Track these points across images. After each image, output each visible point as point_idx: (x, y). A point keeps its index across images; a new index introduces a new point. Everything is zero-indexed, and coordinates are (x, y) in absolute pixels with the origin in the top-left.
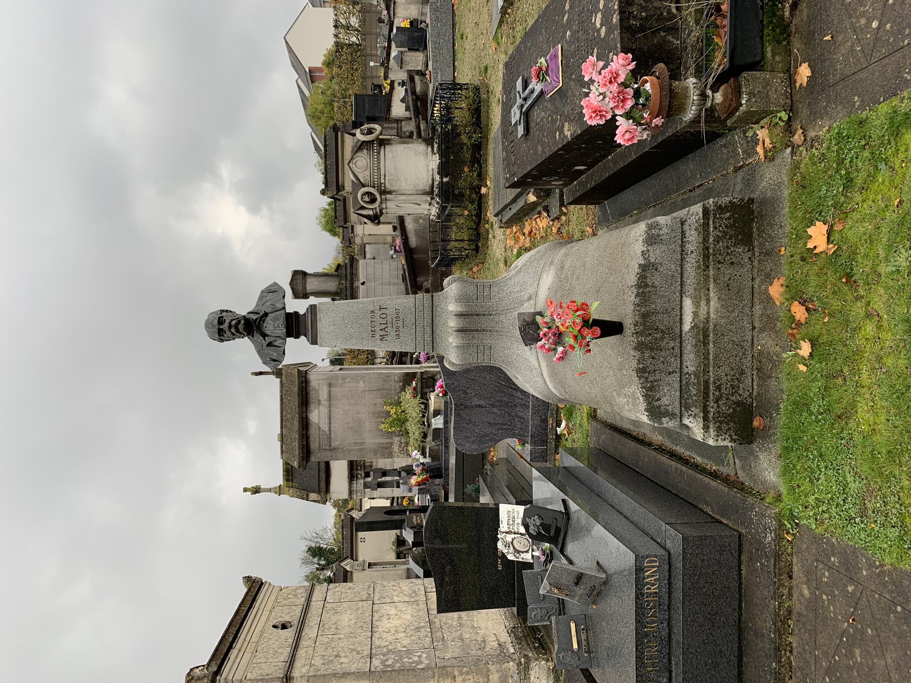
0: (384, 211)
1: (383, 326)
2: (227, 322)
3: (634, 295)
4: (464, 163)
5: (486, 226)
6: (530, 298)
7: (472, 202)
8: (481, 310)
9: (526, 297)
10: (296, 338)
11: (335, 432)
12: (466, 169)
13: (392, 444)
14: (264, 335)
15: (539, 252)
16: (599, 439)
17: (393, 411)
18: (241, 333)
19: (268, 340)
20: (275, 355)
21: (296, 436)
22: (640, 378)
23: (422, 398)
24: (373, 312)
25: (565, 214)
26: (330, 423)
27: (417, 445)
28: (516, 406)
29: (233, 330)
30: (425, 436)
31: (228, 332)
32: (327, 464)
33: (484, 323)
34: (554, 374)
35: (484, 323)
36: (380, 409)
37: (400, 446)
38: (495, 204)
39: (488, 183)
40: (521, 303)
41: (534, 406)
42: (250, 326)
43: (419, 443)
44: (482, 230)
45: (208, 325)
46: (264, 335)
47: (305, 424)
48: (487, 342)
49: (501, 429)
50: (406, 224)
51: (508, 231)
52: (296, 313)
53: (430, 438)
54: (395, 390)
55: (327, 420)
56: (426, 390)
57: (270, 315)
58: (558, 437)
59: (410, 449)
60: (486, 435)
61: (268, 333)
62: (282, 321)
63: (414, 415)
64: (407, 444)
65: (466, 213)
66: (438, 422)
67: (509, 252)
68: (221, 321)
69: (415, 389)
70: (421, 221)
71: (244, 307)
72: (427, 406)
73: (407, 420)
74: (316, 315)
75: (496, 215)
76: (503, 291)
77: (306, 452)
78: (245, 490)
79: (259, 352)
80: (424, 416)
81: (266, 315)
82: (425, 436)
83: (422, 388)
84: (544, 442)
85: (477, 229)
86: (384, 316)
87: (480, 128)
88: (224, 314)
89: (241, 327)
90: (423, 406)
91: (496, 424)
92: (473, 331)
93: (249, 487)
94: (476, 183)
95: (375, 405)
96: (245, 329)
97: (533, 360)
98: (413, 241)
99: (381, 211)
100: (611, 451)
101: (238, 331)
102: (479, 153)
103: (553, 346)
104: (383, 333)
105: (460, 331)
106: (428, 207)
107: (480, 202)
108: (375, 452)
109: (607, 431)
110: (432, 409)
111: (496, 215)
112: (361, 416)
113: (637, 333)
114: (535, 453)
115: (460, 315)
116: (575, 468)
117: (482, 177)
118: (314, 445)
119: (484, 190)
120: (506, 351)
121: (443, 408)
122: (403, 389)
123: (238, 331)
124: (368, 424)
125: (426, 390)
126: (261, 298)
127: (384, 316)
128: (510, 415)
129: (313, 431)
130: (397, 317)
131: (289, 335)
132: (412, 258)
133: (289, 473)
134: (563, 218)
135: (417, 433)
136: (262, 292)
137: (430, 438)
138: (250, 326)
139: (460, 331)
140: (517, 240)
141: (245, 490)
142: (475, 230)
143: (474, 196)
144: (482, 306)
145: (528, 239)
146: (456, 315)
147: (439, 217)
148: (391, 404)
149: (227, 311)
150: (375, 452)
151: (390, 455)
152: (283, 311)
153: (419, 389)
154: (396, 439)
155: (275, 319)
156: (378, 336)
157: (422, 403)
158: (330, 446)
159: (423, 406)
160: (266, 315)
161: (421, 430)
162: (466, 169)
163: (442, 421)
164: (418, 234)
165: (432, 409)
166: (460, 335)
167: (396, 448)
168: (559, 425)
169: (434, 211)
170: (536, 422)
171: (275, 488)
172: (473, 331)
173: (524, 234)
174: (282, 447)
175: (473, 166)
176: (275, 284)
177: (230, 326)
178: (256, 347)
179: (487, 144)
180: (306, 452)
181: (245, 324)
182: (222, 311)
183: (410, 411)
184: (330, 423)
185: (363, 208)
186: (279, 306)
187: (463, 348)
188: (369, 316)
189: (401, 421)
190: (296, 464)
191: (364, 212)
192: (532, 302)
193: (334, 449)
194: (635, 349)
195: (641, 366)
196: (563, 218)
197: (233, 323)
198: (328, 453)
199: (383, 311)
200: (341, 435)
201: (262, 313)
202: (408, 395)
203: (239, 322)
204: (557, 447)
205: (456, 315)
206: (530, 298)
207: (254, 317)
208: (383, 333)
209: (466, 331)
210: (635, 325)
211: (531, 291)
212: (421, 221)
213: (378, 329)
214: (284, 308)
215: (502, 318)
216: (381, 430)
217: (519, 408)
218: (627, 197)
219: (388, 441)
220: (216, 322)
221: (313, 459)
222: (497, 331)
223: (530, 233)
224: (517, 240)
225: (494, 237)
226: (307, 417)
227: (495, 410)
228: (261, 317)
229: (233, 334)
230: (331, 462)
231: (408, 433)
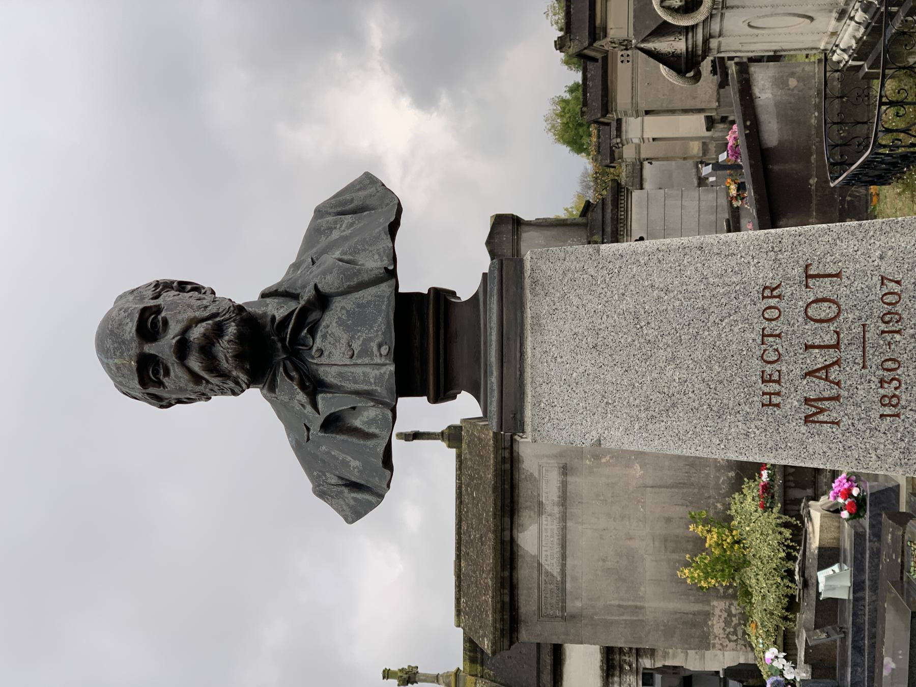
0: (714, 43)
1: (819, 359)
2: (175, 329)
10: (436, 399)
11: (574, 579)
13: (708, 615)
14: (313, 386)
17: (711, 539)
18: (224, 375)
19: (327, 404)
20: (355, 468)
21: (489, 581)
23: (784, 511)
24: (770, 291)
26: (564, 557)
27: (770, 626)
29: (195, 363)
30: (792, 605)
31: (176, 370)
32: (558, 653)
36: (679, 531)
37: (727, 623)
42: (260, 347)
43: (777, 620)
45: (108, 341)
46: (313, 386)
47: (508, 555)
50: (756, 91)
52: (441, 298)
53: (806, 615)
54: (717, 487)
55: (557, 549)
56: (796, 493)
57: (339, 306)
59: (751, 630)
61: (329, 375)
62: (379, 330)
63: (766, 552)
64: (745, 618)
66: (833, 582)
68: (149, 324)
69: (766, 488)
70: (793, 82)
71: (247, 268)
72: (799, 534)
73: (746, 563)
74: (519, 305)
77: (509, 620)
78: (387, 674)
79: (298, 448)
80: (790, 558)
81: (322, 301)
82: (792, 605)
83: (785, 487)
86: (826, 311)
88: (168, 297)
89: (224, 349)
90: (787, 533)
93: (394, 668)
95: (668, 520)
96: (239, 357)
98: (772, 132)
99: (706, 41)
101: (212, 366)
104: (817, 388)
106: (832, 24)
108: (668, 632)
110: (814, 543)
112: (635, 544)
118: (527, 604)
121: (847, 544)
122: (737, 486)
123: (212, 366)
124: (651, 566)
125: (796, 493)
126: (314, 234)
127: (826, 311)
129: (525, 573)
130: (891, 318)
131: (407, 385)
132: (767, 173)
133: (473, 651)
135: (771, 597)
136: (320, 212)
137: (806, 615)
138: (260, 347)
141: (387, 674)
147: (862, 51)
148: (706, 522)
149: (182, 286)
150: (668, 632)
151: (704, 643)
152: (385, 288)
153: (777, 489)
154: (719, 606)
155: (356, 321)
156: (794, 402)
157: (786, 525)
158: (564, 609)
159: (787, 533)
160: (322, 301)
161: (783, 591)
163: (847, 582)
164: (785, 113)
165: (814, 543)
167: (717, 626)
169: (849, 34)
171: (447, 675)
174: (458, 600)
176: (369, 181)
177: (182, 348)
178: (289, 428)
180: (509, 620)
181: (240, 338)
182: (162, 287)
183: (754, 540)
184: (564, 557)
185: (664, 30)
186: (372, 264)
188: (752, 310)
189: (732, 565)
190: (486, 645)
191: (664, 45)
193: (573, 617)
197: (197, 333)
198: (560, 626)
199: (824, 288)
200: (588, 585)
201: (307, 294)
202: (748, 502)
203: (218, 330)
207: (278, 310)
208: (817, 388)
212: (793, 82)
213: (792, 368)
214: (391, 274)
216: (684, 581)
219: (698, 607)
220: (131, 328)
221: (524, 635)
226: (512, 541)
228: (304, 312)
229: (197, 379)
230: (566, 645)
231: (748, 594)
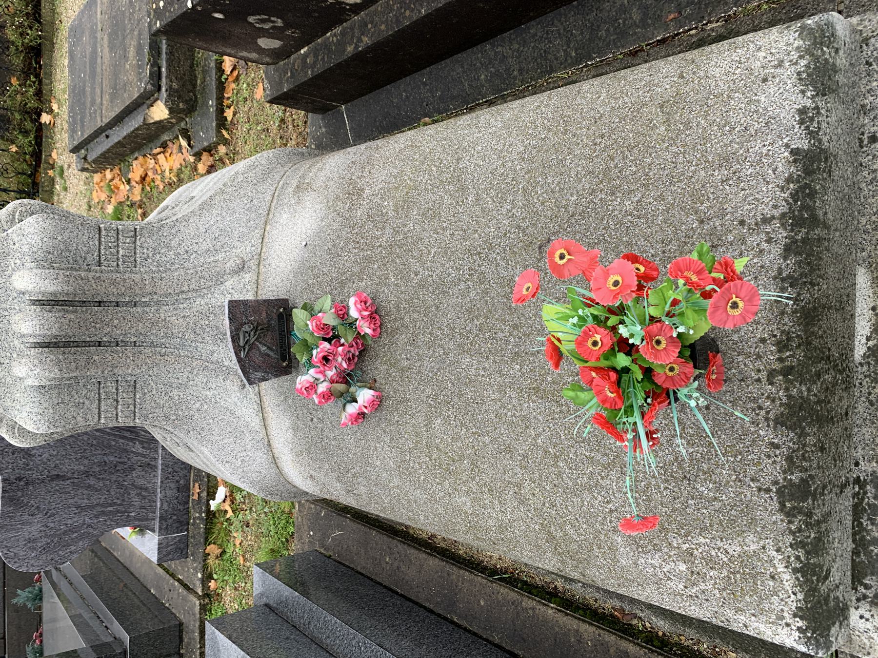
3: (776, 250)
4: (10, 71)
5: (51, 173)
6: (242, 268)
7: (26, 133)
8: (112, 293)
9: (230, 265)
12: (14, 81)
15: (253, 167)
16: (325, 536)
22: (790, 514)
25: (226, 142)
28: (132, 468)
33: (116, 324)
34: (313, 448)
35: (116, 324)
38: (72, 131)
39: (55, 107)
40: (219, 279)
41: (165, 466)
44: (42, 177)
48: (127, 372)
49: (103, 513)
51: (97, 177)
58: (211, 516)
60: (72, 531)
65: (14, 149)
67: (96, 212)
75: (75, 150)
76: (169, 247)
84: (183, 524)
85: (34, 174)
87: (40, 22)
91: (92, 507)
92: (89, 344)
94: (32, 104)
97: (248, 413)
100: (362, 563)
102: (38, 63)
103: (341, 387)
105: (48, 344)
107: (40, 137)
109: (336, 519)
111: (75, 150)
113: (787, 372)
114: (168, 545)
115: (49, 302)
116: (284, 602)
117: (42, 96)
119: (45, 118)
120: (175, 393)
128: (120, 486)
134: (222, 149)
139: (48, 344)
140: (113, 191)
142: (30, 176)
143: (28, 125)
144: (114, 282)
145: (138, 189)
146: (35, 302)
162: (14, 81)
166: (51, 356)
168: (212, 495)
170: (169, 493)
172: (89, 344)
173: (129, 182)
175: (27, 77)
179: (52, 51)
187: (55, 392)
192: (248, 277)
194: (780, 421)
195: (795, 477)
196: (222, 149)
204: (208, 531)
205: (35, 302)
206: (242, 268)
209: (67, 345)
210: (782, 346)
211: (245, 249)
215: (165, 312)
217: (138, 472)
218: (400, 92)
222: (152, 345)
223: (143, 179)
224: (113, 191)
225: (66, 189)
227: (92, 481)
